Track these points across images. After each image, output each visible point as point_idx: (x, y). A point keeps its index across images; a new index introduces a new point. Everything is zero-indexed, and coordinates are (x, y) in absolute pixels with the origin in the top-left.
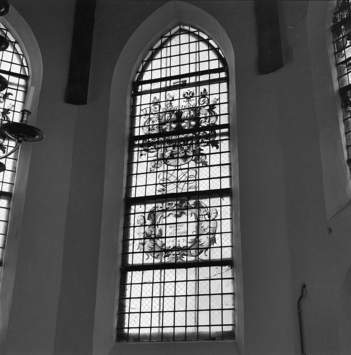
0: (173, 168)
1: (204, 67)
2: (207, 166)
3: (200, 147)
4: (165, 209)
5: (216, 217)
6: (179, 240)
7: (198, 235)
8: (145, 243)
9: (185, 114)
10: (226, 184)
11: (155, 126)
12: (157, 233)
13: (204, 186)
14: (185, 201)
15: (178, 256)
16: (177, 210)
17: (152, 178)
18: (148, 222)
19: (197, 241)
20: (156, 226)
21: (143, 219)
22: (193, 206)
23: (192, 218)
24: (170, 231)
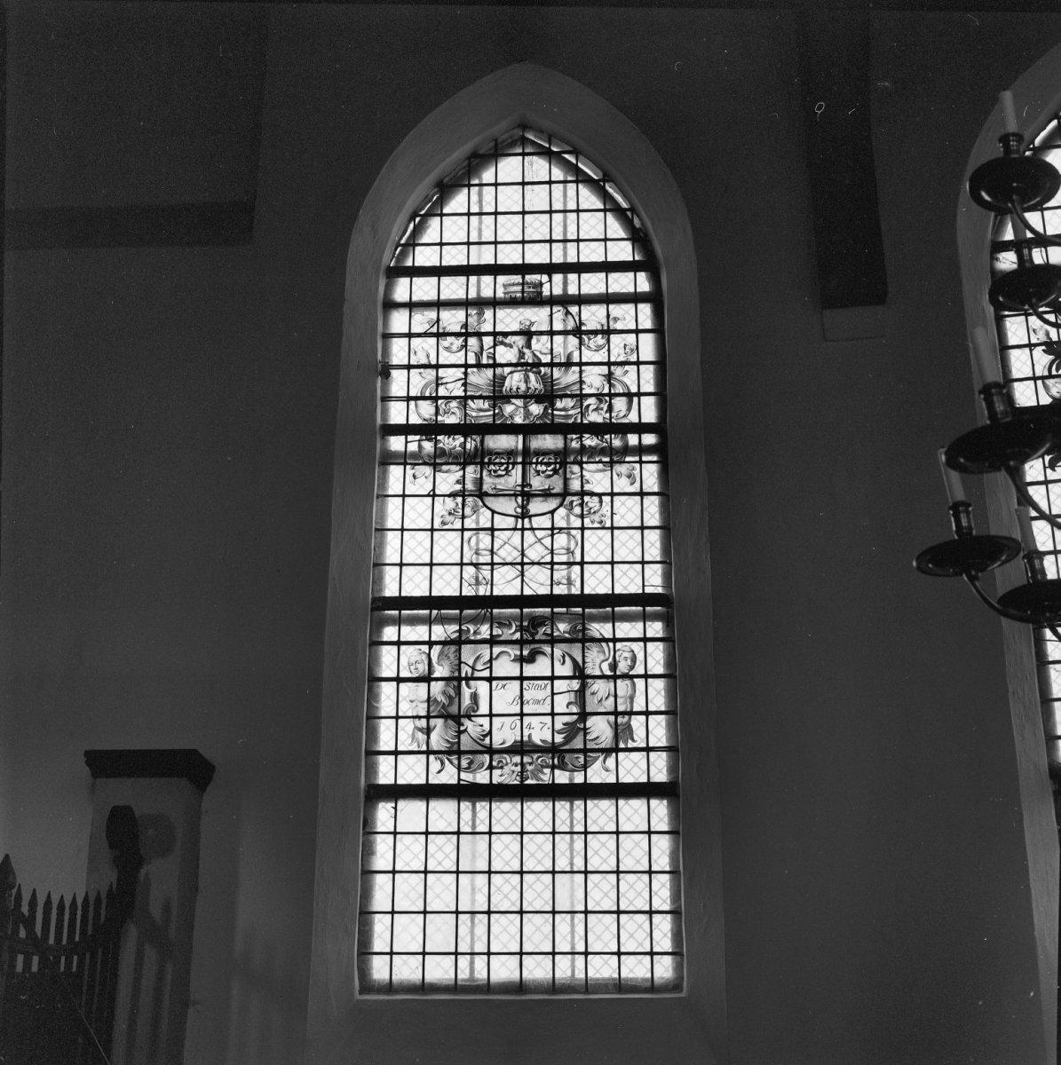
0: (510, 522)
1: (592, 253)
2: (603, 528)
4: (489, 637)
5: (632, 668)
6: (529, 724)
7: (584, 715)
8: (432, 727)
10: (654, 581)
11: (454, 404)
12: (466, 701)
13: (597, 583)
14: (545, 621)
15: (529, 768)
16: (521, 643)
19: (577, 727)
20: (464, 682)
21: (426, 662)
22: (567, 635)
23: (566, 670)
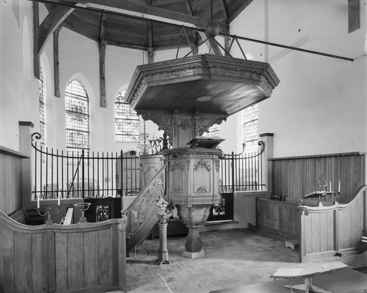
7: (82, 142)
9: (78, 108)
17: (71, 124)
18: (71, 136)
23: (81, 137)
24: (76, 139)
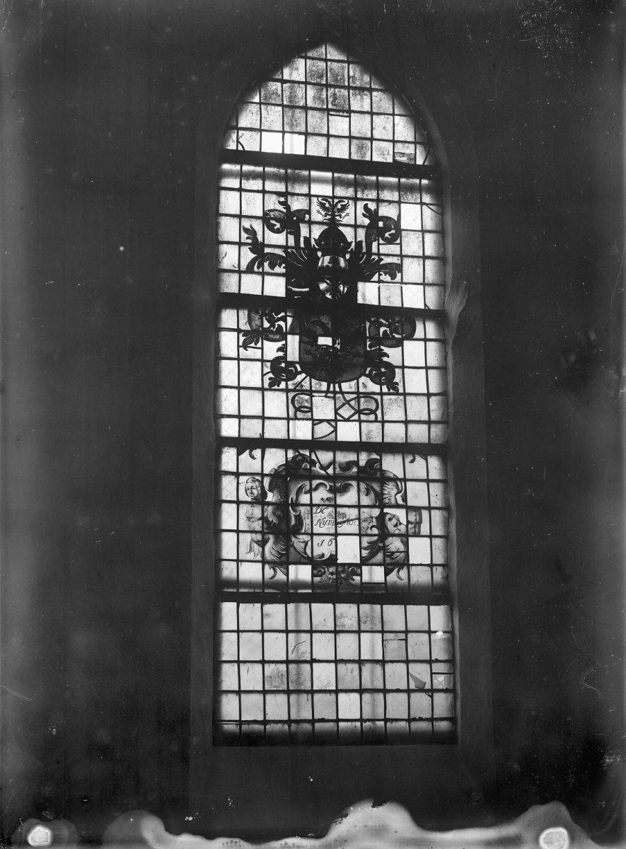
2: (397, 394)
3: (382, 347)
12: (293, 522)
21: (259, 489)
